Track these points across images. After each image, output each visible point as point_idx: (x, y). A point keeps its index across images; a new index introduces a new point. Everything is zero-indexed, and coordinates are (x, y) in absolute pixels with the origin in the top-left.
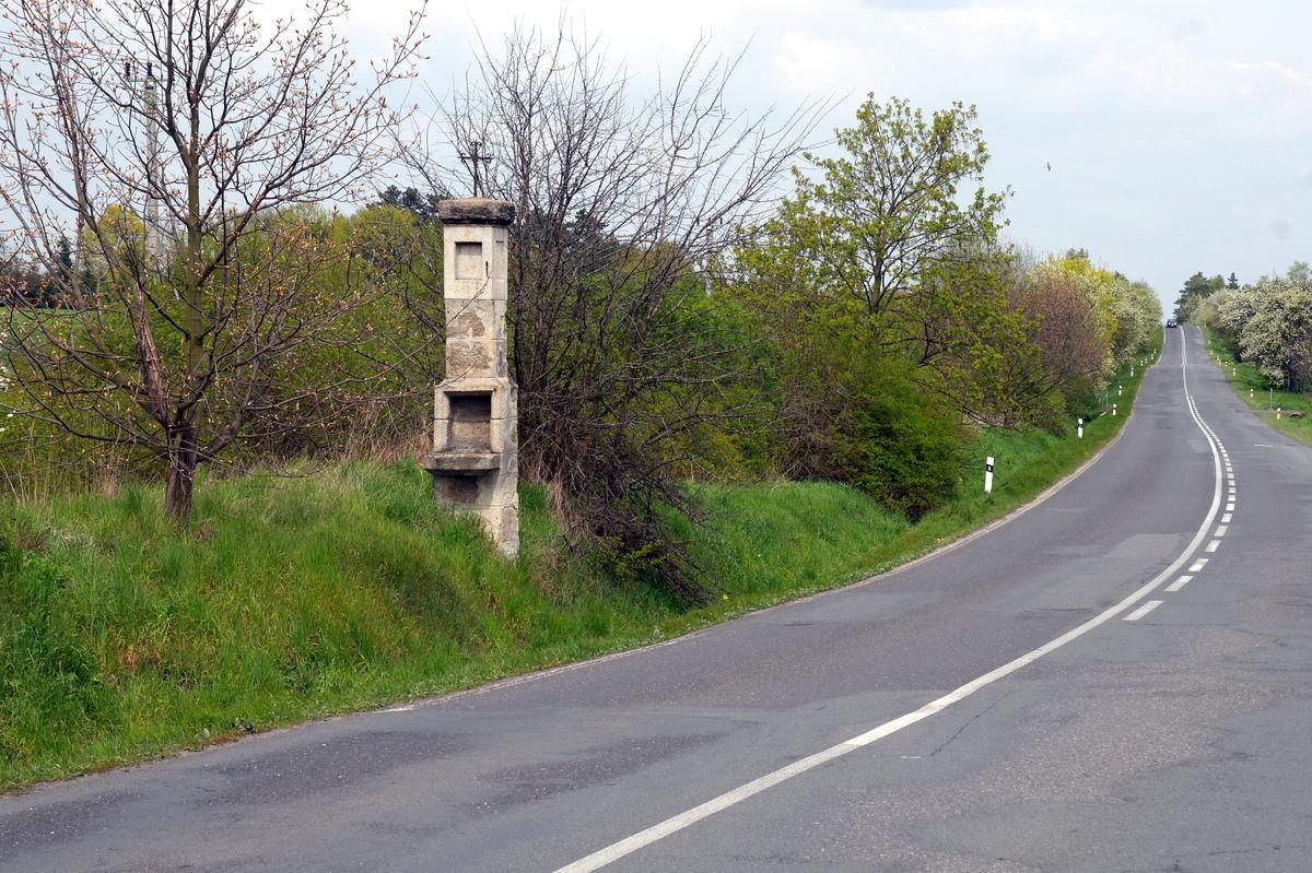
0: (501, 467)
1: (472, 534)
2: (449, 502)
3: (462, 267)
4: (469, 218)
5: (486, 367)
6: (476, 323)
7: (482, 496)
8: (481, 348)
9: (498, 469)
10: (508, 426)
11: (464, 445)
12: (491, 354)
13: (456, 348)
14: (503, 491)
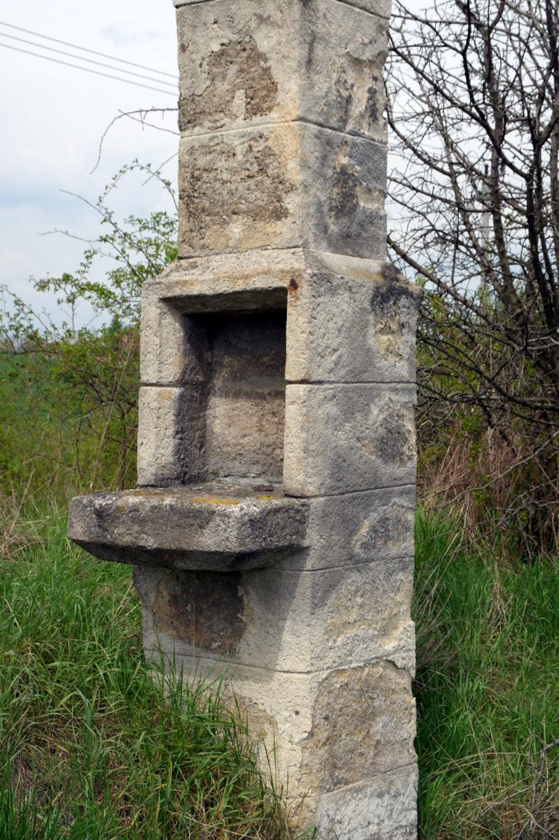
0: (313, 538)
1: (210, 759)
2: (168, 642)
5: (280, 214)
6: (255, 71)
7: (252, 634)
8: (268, 152)
9: (296, 551)
10: (350, 410)
11: (237, 467)
12: (294, 172)
13: (202, 161)
14: (327, 617)
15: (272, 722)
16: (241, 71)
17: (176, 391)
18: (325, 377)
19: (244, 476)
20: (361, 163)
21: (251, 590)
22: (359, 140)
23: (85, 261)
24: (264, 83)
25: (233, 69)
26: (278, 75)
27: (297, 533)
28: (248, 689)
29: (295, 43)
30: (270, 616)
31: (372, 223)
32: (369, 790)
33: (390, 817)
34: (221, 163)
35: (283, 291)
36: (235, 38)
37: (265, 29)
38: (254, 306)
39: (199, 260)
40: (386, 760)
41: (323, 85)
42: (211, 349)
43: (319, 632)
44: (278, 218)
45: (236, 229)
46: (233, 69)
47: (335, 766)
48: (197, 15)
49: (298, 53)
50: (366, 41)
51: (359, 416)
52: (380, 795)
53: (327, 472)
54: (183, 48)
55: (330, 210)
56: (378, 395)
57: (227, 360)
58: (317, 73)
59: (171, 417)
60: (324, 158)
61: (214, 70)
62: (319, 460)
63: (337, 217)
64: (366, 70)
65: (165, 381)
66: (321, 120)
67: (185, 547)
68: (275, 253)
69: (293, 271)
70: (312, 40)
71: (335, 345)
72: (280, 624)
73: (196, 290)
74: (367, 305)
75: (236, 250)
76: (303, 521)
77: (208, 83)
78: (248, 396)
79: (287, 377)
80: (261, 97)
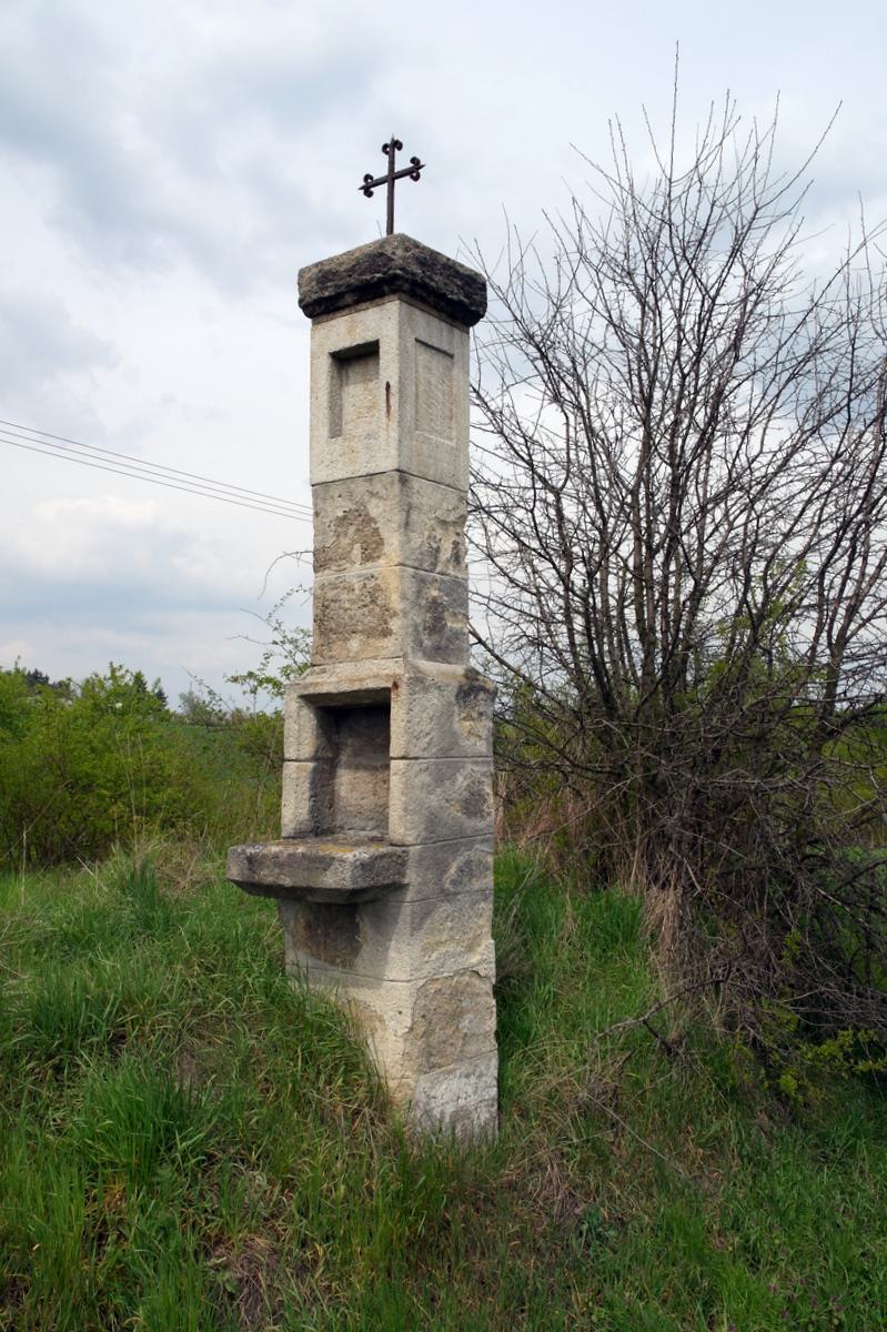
0: (412, 877)
1: (334, 1050)
3: (349, 411)
4: (353, 289)
5: (386, 633)
6: (368, 531)
7: (366, 951)
8: (377, 588)
9: (398, 887)
11: (358, 822)
12: (396, 603)
13: (330, 594)
14: (423, 938)
15: (381, 1020)
16: (358, 530)
17: (311, 765)
18: (420, 754)
19: (363, 829)
20: (447, 595)
21: (366, 919)
22: (446, 578)
23: (264, 661)
24: (374, 539)
25: (352, 529)
26: (384, 533)
27: (399, 873)
28: (362, 994)
29: (396, 511)
30: (379, 938)
31: (457, 638)
32: (458, 1072)
33: (475, 1093)
34: (344, 596)
35: (388, 690)
36: (353, 507)
37: (374, 501)
38: (367, 701)
39: (328, 667)
40: (472, 1048)
41: (417, 540)
42: (338, 733)
43: (416, 949)
44: (385, 636)
45: (355, 644)
46: (352, 529)
47: (431, 1055)
48: (327, 491)
49: (398, 518)
50: (450, 508)
51: (447, 783)
52: (467, 1076)
53: (423, 826)
54: (317, 514)
55: (425, 629)
56: (463, 767)
57: (350, 741)
58: (413, 532)
59: (307, 785)
60: (419, 592)
61: (339, 529)
62: (416, 818)
63: (429, 635)
64: (451, 528)
65: (302, 757)
66: (416, 565)
67: (312, 885)
68: (383, 662)
69: (395, 676)
70: (409, 509)
71: (427, 730)
72: (387, 944)
73: (324, 689)
74: (453, 699)
75: (355, 659)
76: (403, 864)
77: (335, 538)
78: (365, 768)
79: (392, 755)
80: (372, 550)
